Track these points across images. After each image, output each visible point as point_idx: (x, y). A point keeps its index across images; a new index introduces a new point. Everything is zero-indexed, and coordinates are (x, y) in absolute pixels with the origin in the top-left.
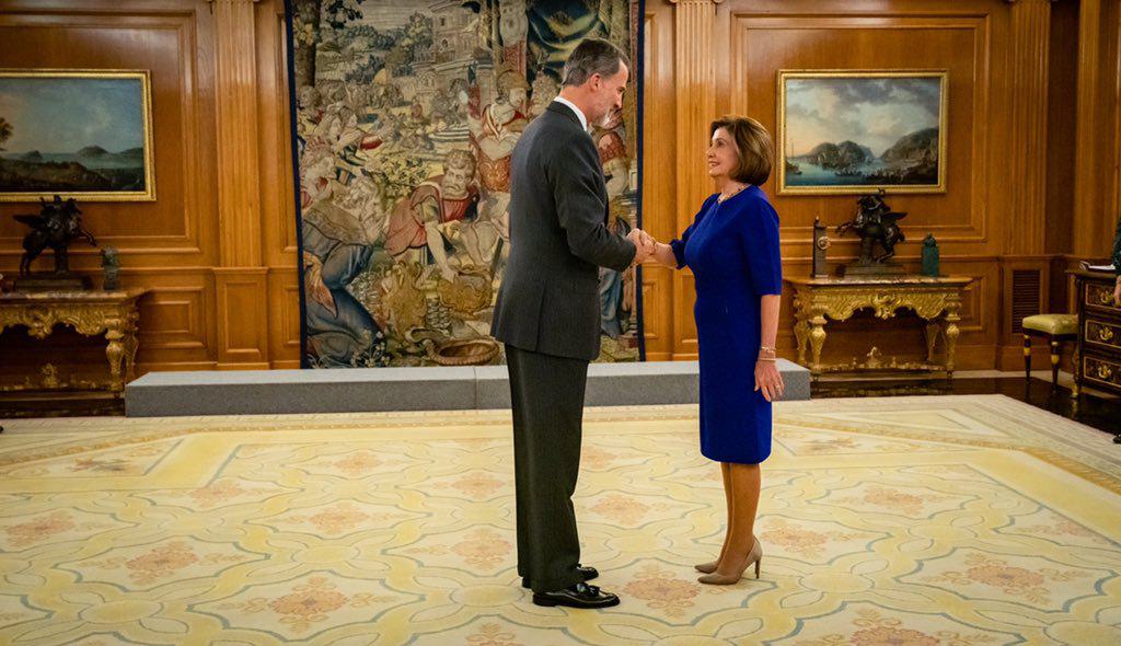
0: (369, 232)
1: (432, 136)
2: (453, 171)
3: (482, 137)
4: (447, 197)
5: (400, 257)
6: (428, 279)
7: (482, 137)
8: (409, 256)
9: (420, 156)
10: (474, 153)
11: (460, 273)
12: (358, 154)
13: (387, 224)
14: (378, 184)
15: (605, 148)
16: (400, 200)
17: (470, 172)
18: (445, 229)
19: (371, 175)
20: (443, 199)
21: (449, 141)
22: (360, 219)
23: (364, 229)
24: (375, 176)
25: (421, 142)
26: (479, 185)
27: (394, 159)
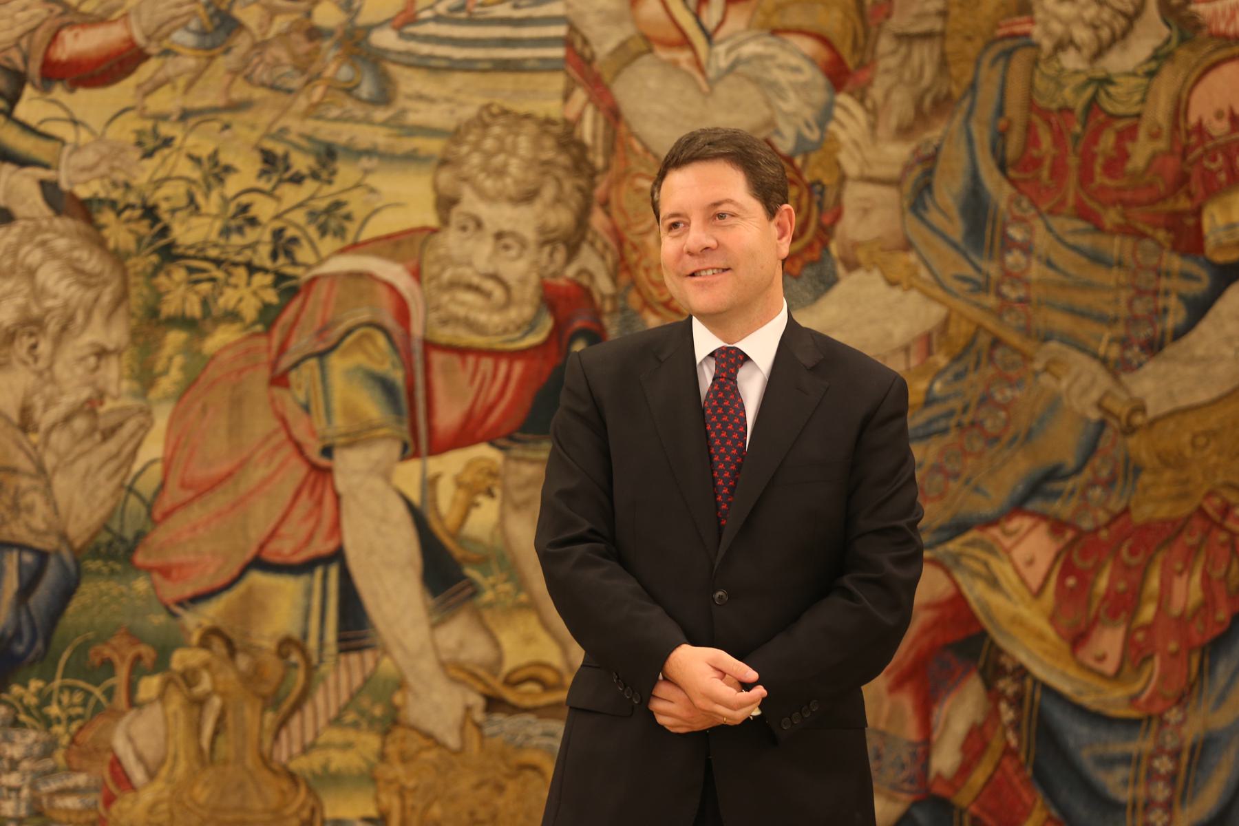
0: (61, 484)
1: (385, 39)
2: (483, 210)
3: (626, 55)
4: (445, 335)
5: (211, 612)
6: (336, 722)
7: (626, 55)
8: (251, 607)
9: (328, 131)
10: (587, 131)
11: (494, 703)
12: (30, 107)
13: (153, 448)
14: (118, 258)
15: (1219, 128)
16: (221, 338)
17: (562, 218)
18: (429, 484)
19: (85, 210)
20: (429, 345)
21: (467, 66)
22: (26, 423)
23: (41, 469)
24: (107, 217)
25: (336, 68)
26: (604, 285)
27: (201, 142)
